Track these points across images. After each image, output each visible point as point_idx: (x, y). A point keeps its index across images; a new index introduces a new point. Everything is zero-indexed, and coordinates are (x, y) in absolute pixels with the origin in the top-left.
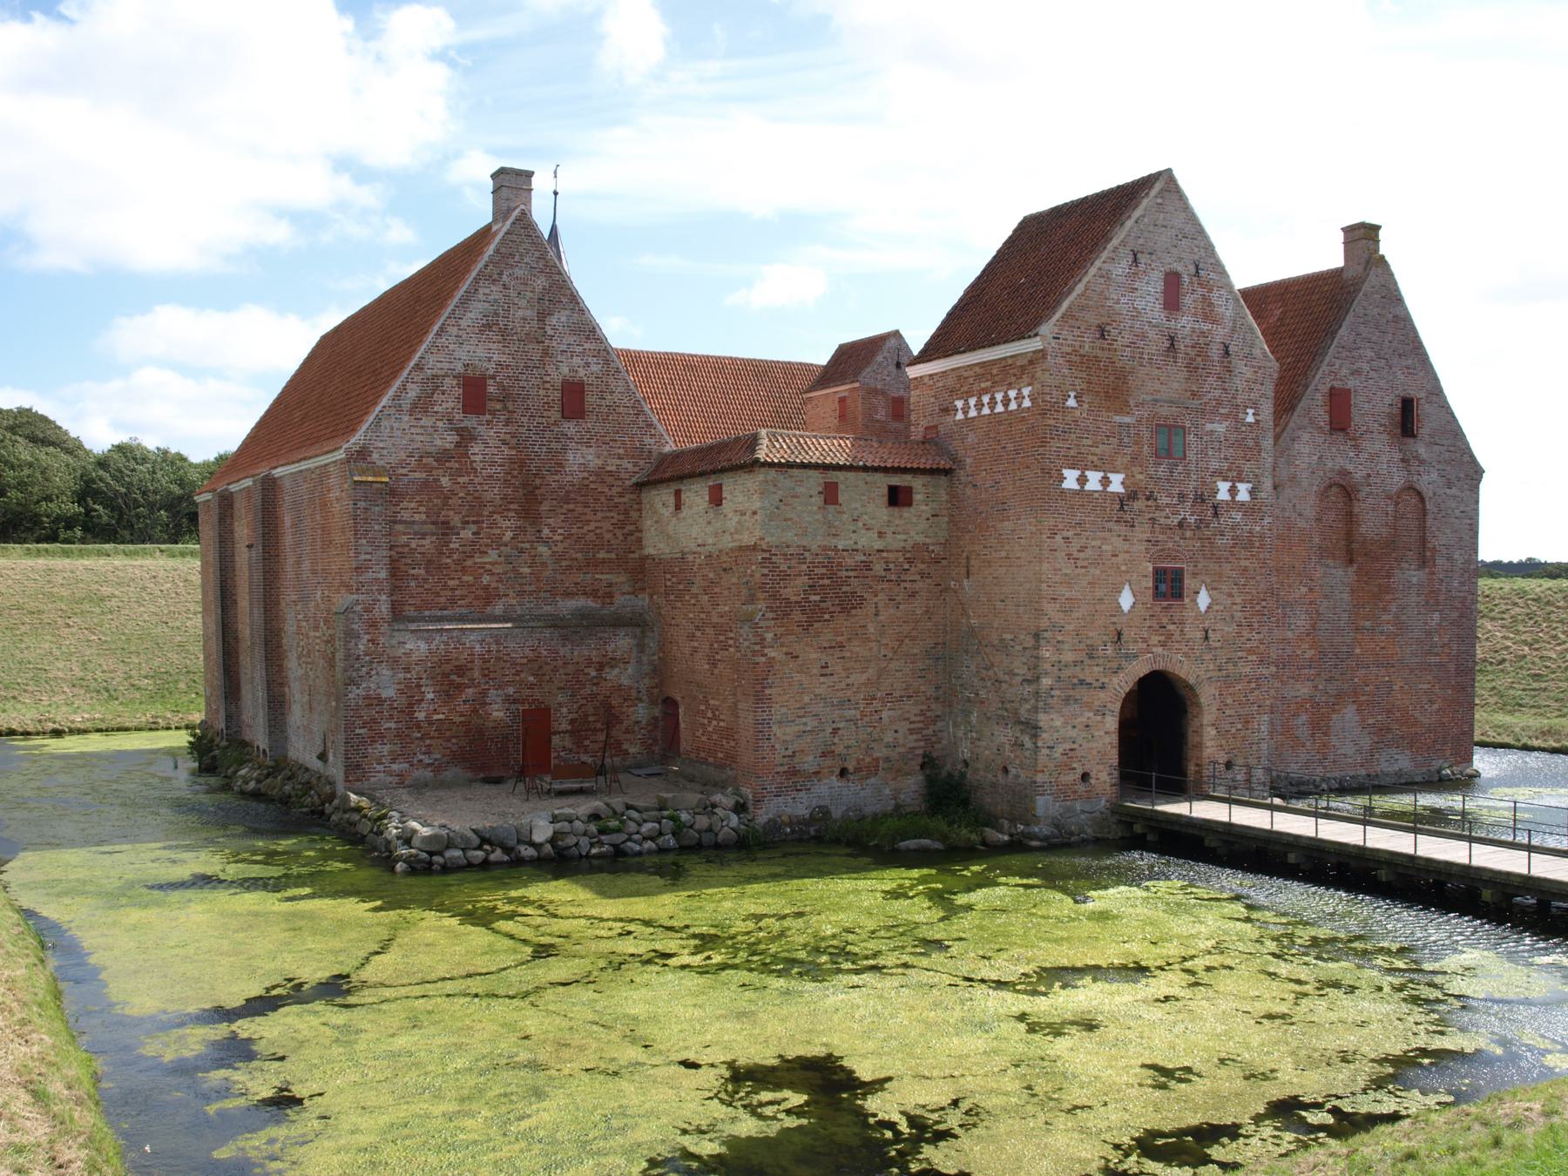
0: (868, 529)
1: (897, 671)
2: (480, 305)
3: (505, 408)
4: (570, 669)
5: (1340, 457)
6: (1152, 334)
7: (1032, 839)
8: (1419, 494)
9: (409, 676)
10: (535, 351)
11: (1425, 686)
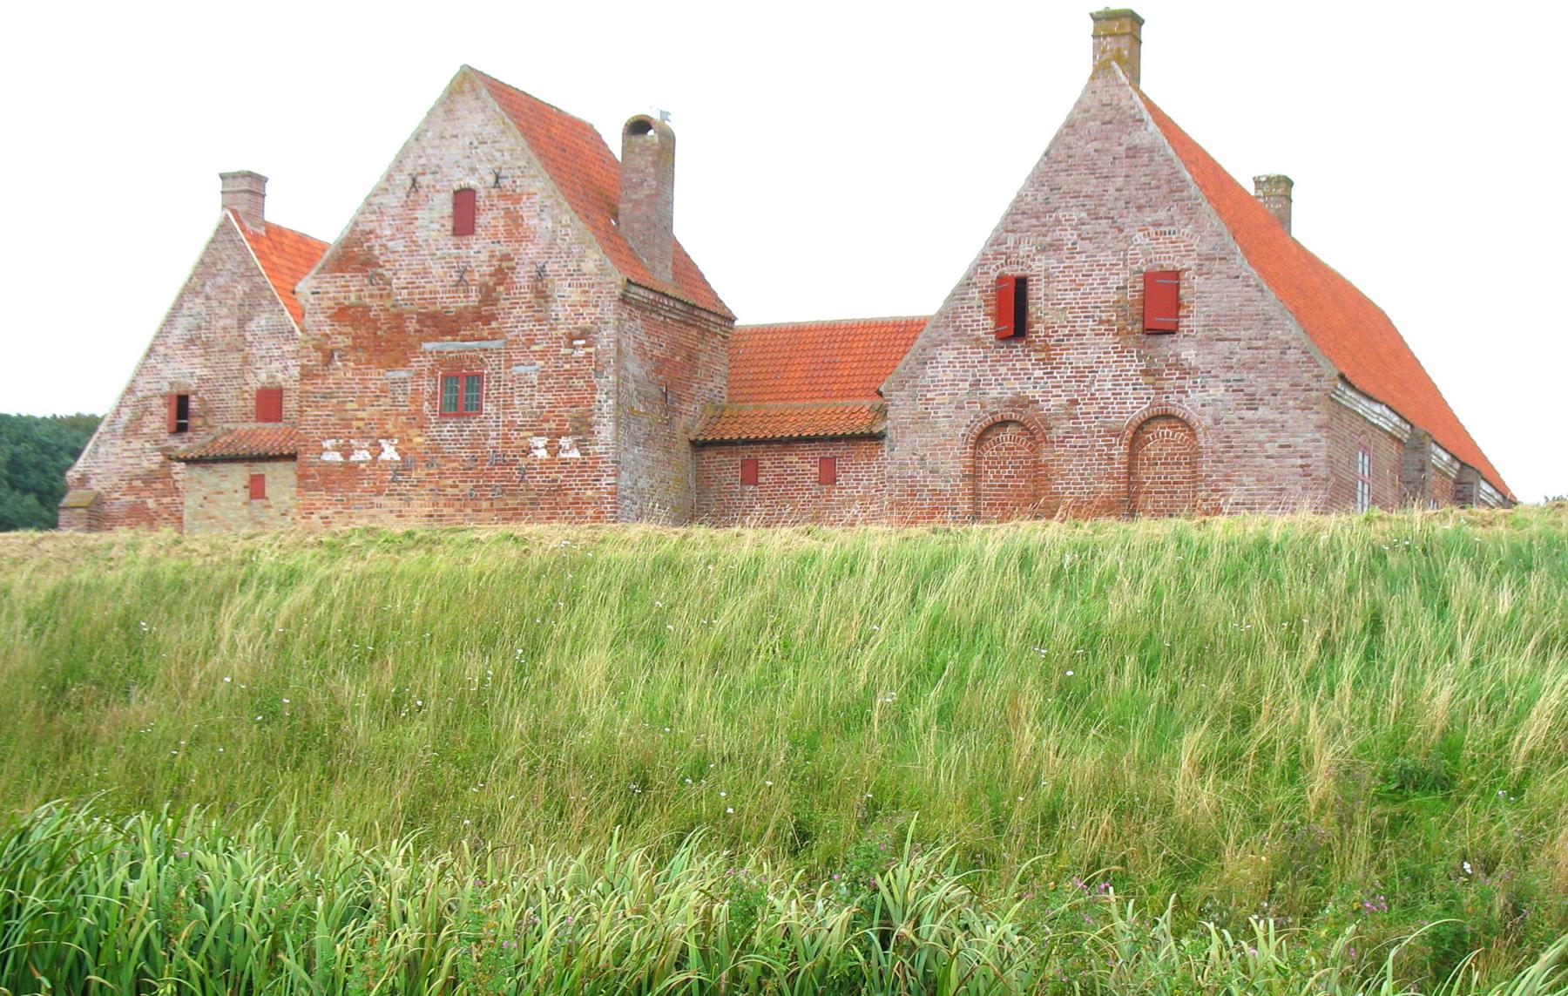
2: (183, 320)
3: (206, 424)
6: (437, 270)
8: (1184, 423)
10: (235, 360)
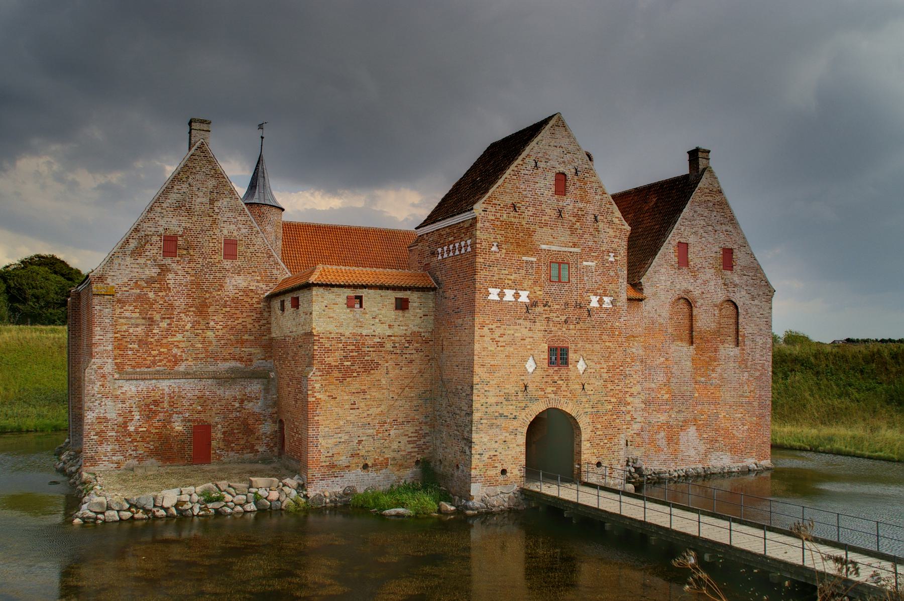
0: (381, 323)
1: (400, 407)
3: (189, 253)
4: (224, 402)
5: (684, 283)
7: (469, 510)
9: (124, 405)
11: (740, 415)
